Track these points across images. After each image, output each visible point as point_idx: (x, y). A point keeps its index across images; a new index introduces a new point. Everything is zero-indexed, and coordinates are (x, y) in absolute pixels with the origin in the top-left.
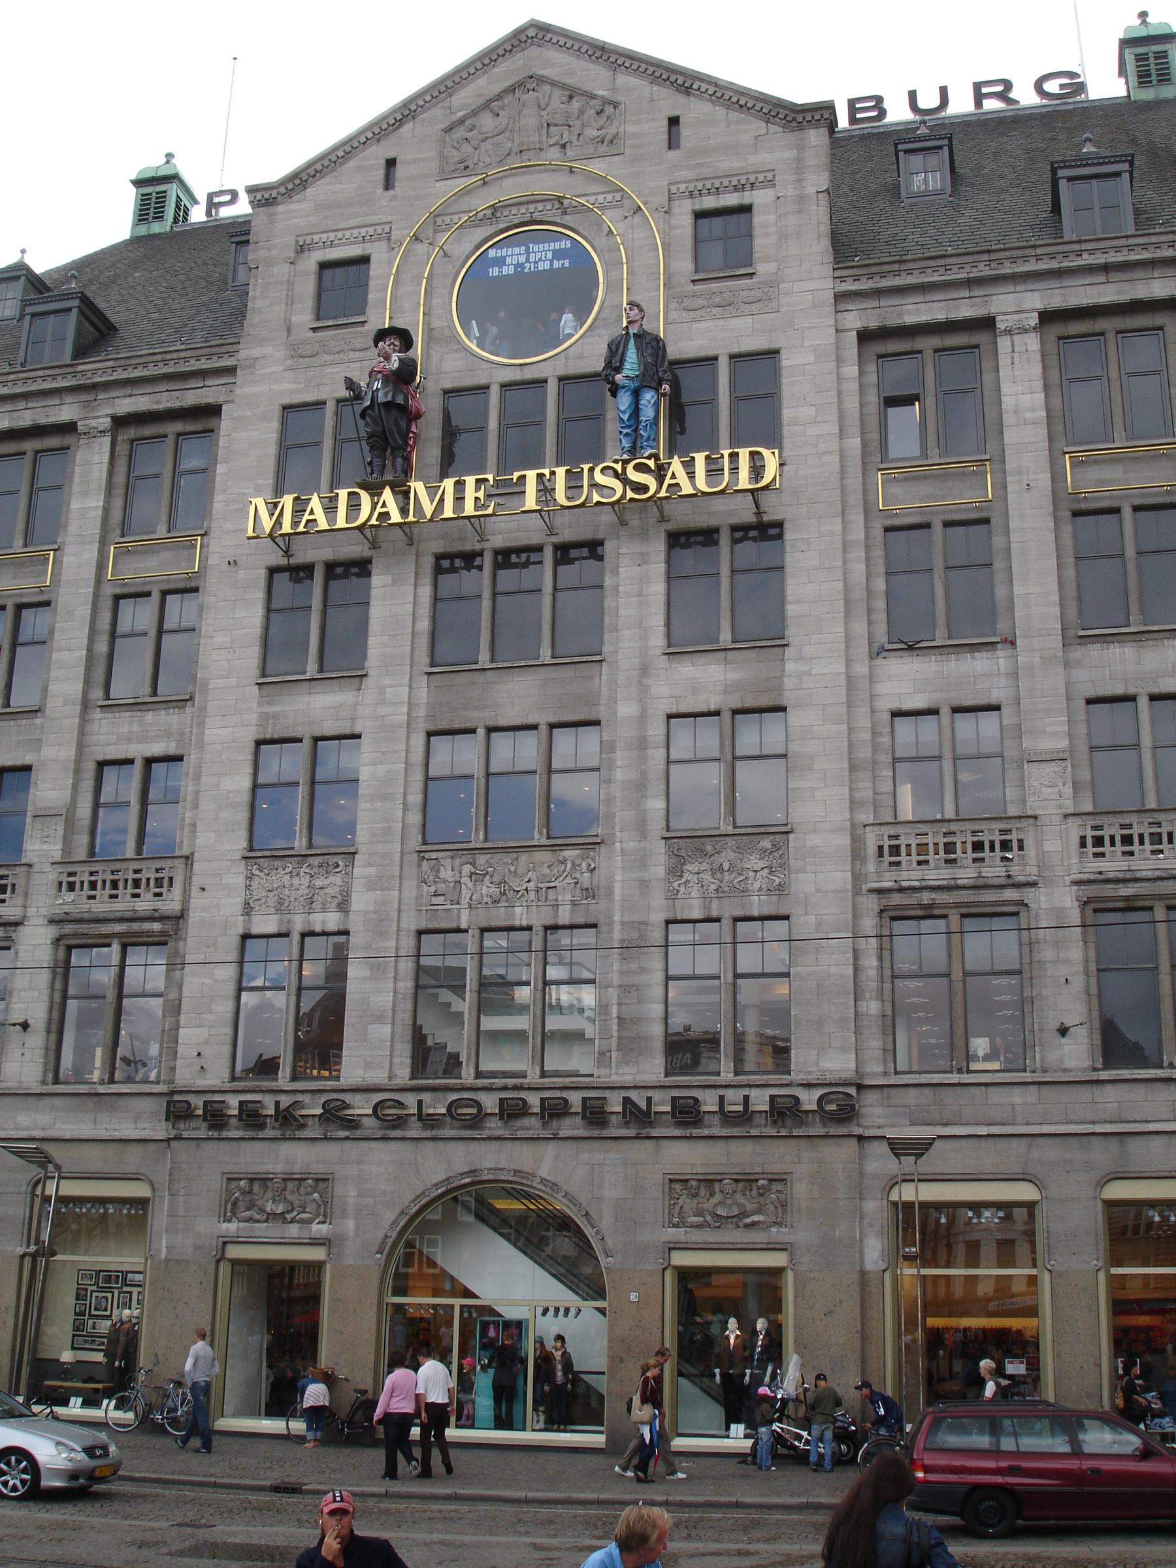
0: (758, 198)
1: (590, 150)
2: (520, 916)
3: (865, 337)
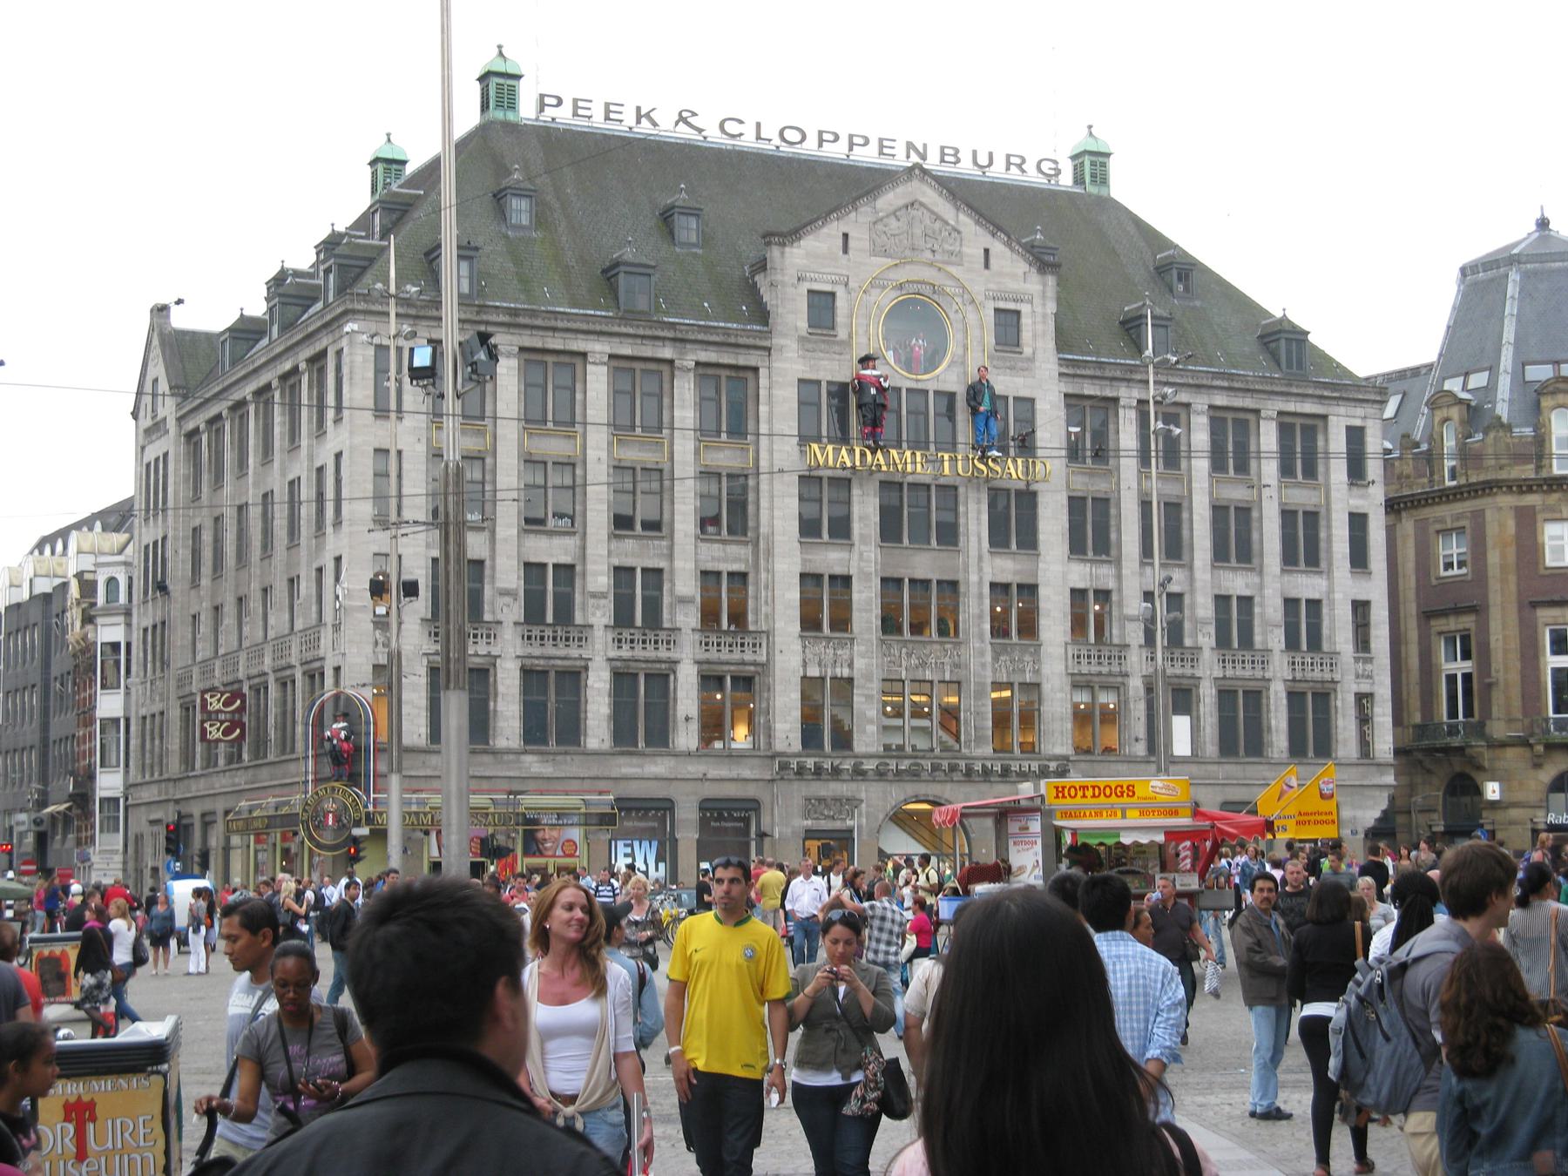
0: (1025, 309)
1: (946, 258)
2: (928, 675)
3: (1066, 395)
